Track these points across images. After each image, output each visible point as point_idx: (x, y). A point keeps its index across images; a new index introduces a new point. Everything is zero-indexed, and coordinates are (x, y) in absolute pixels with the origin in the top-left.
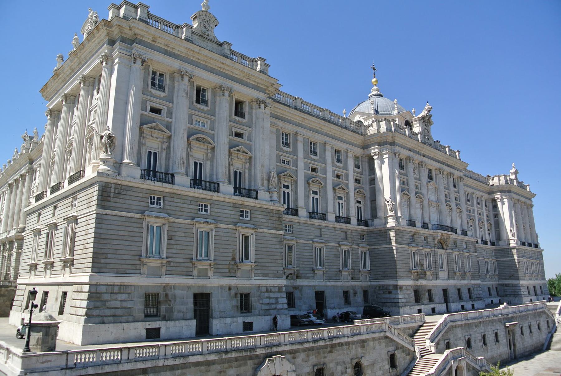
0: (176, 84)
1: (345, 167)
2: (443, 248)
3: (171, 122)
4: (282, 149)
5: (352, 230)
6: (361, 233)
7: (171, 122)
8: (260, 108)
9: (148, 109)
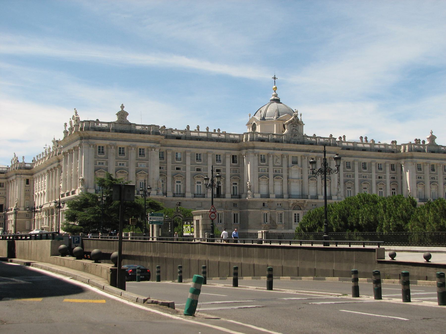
0: (109, 150)
1: (224, 165)
2: (301, 209)
3: (108, 167)
4: (176, 162)
5: (226, 201)
6: (234, 202)
7: (108, 167)
8: (152, 150)
9: (98, 164)
